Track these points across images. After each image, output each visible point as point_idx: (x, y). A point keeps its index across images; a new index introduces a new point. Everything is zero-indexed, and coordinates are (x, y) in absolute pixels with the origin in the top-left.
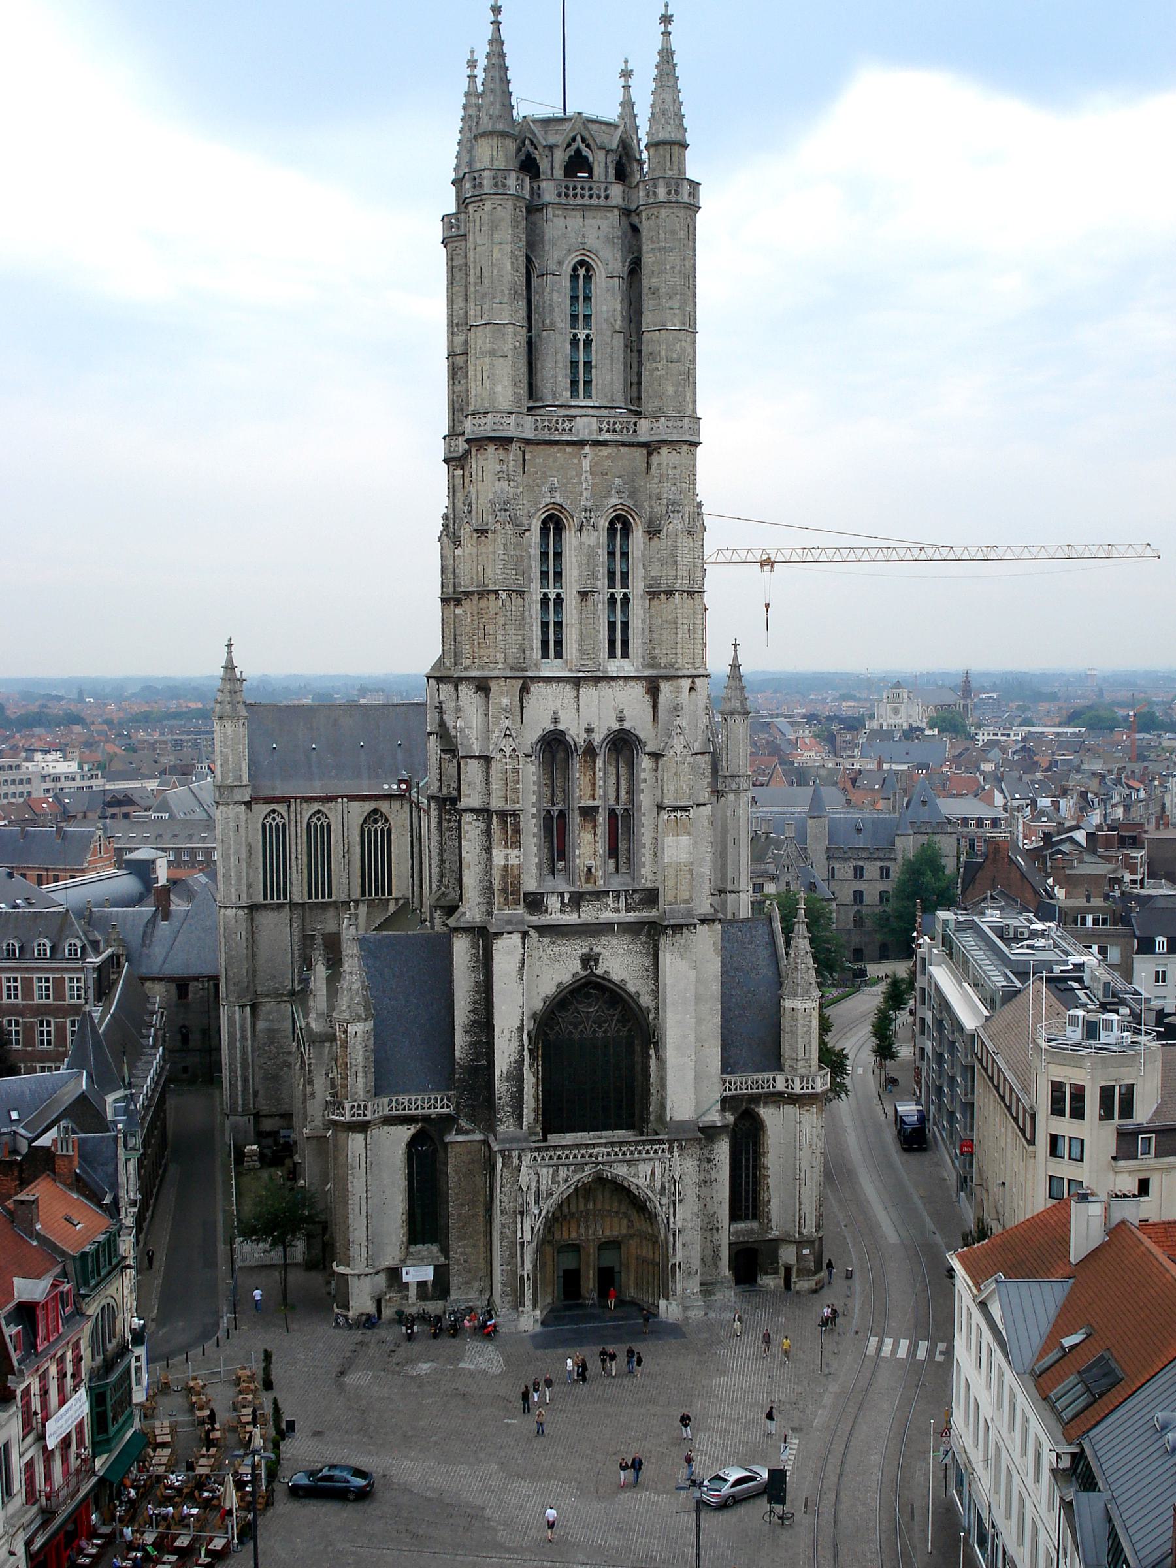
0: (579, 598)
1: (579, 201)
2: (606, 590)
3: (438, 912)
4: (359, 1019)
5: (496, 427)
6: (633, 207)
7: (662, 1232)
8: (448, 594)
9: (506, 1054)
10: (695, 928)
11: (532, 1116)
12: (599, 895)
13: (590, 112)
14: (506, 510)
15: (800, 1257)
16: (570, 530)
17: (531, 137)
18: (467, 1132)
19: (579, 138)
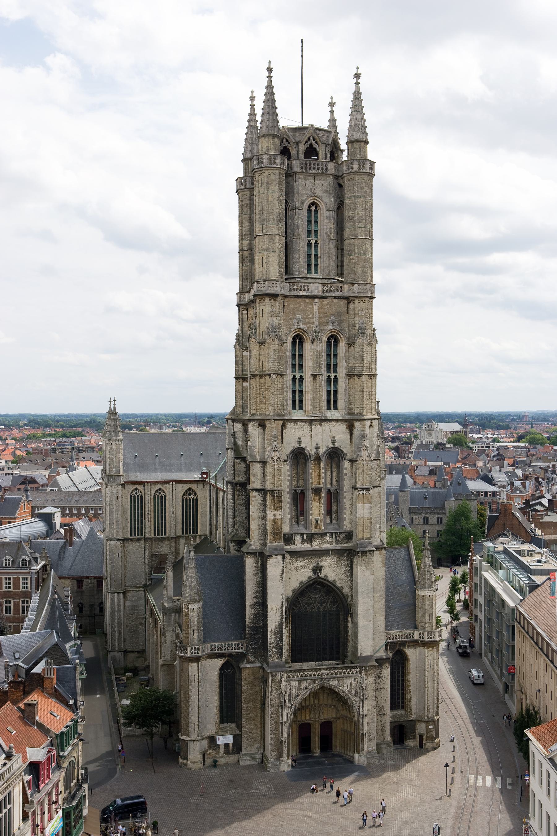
0: (312, 378)
1: (312, 171)
2: (326, 374)
3: (233, 543)
4: (195, 601)
5: (270, 289)
6: (340, 174)
7: (356, 716)
8: (239, 375)
9: (274, 621)
10: (373, 552)
11: (286, 653)
12: (322, 535)
13: (317, 125)
14: (275, 332)
15: (427, 730)
16: (308, 342)
17: (286, 137)
18: (252, 662)
19: (312, 138)
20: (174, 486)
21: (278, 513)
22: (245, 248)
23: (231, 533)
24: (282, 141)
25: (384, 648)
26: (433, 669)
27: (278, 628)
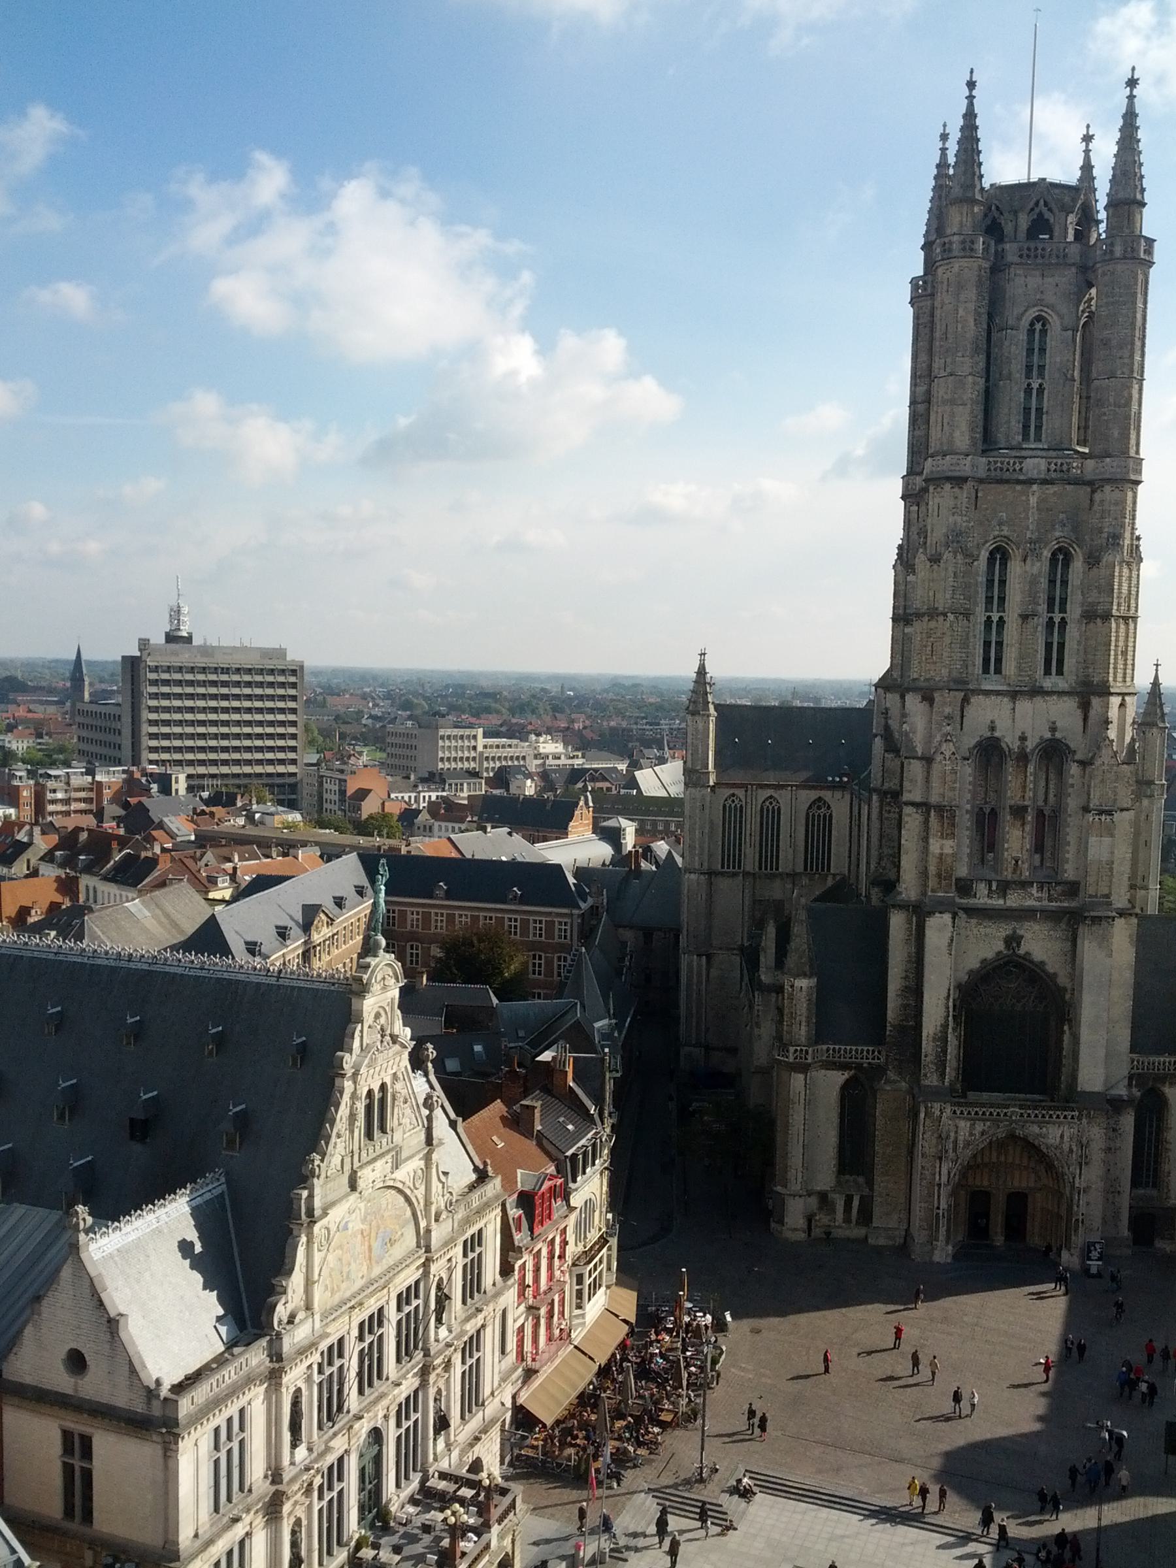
0: (1020, 621)
4: (805, 975)
5: (953, 468)
7: (1068, 1190)
11: (954, 1074)
12: (1024, 885)
14: (958, 542)
17: (996, 202)
19: (1042, 202)
24: (990, 208)
25: (1126, 1082)
27: (941, 1032)
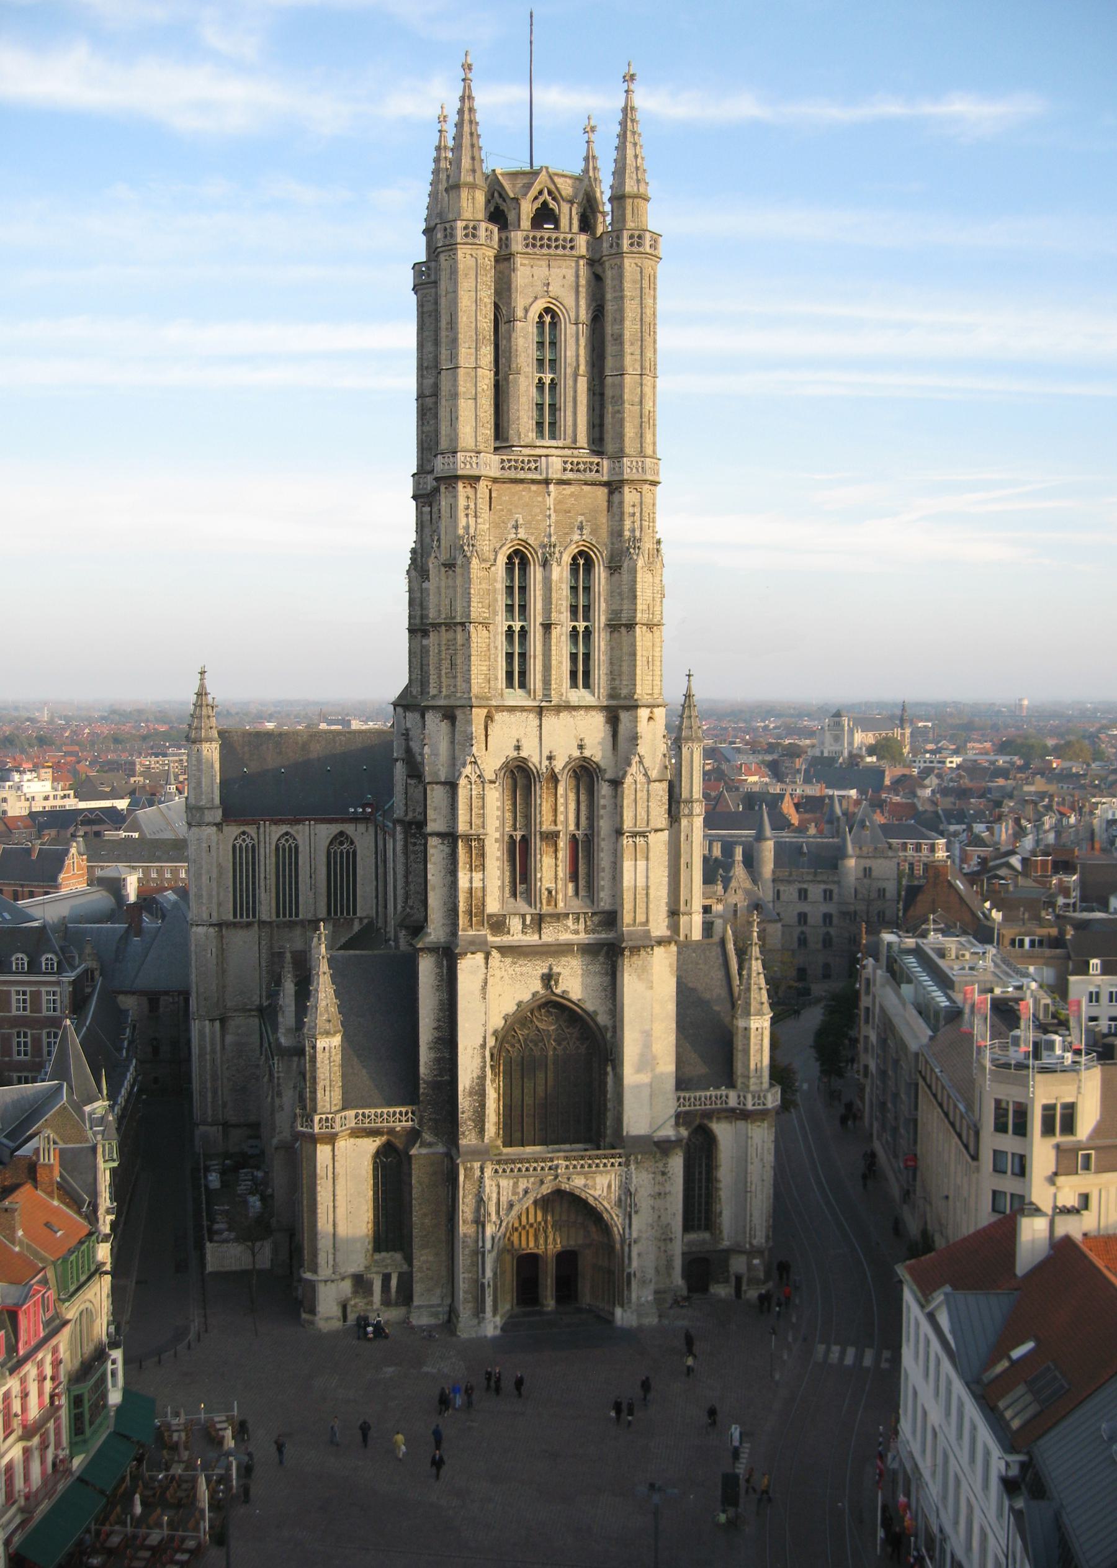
3: (404, 932)
6: (597, 257)
8: (415, 625)
9: (469, 1072)
10: (652, 950)
12: (558, 917)
15: (750, 1267)
17: (499, 189)
18: (430, 1145)
20: (312, 827)
21: (477, 876)
22: (427, 393)
23: (401, 912)
24: (493, 196)
25: (673, 1121)
26: (762, 1160)
27: (477, 1084)
